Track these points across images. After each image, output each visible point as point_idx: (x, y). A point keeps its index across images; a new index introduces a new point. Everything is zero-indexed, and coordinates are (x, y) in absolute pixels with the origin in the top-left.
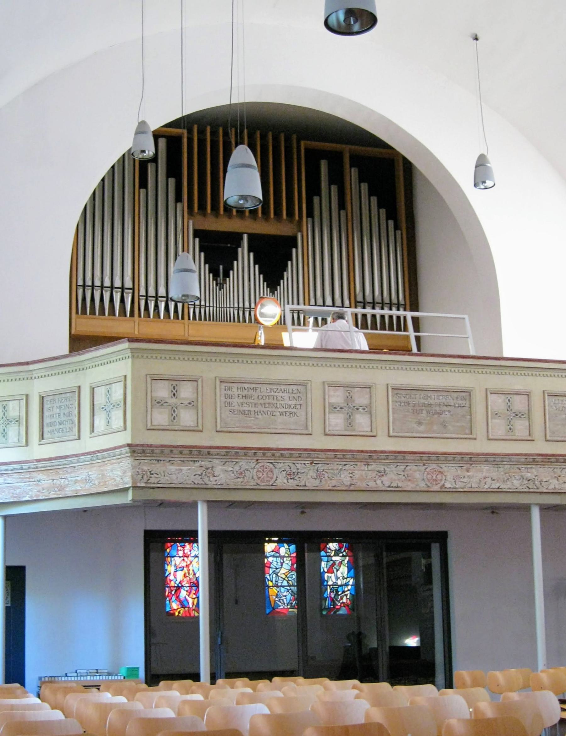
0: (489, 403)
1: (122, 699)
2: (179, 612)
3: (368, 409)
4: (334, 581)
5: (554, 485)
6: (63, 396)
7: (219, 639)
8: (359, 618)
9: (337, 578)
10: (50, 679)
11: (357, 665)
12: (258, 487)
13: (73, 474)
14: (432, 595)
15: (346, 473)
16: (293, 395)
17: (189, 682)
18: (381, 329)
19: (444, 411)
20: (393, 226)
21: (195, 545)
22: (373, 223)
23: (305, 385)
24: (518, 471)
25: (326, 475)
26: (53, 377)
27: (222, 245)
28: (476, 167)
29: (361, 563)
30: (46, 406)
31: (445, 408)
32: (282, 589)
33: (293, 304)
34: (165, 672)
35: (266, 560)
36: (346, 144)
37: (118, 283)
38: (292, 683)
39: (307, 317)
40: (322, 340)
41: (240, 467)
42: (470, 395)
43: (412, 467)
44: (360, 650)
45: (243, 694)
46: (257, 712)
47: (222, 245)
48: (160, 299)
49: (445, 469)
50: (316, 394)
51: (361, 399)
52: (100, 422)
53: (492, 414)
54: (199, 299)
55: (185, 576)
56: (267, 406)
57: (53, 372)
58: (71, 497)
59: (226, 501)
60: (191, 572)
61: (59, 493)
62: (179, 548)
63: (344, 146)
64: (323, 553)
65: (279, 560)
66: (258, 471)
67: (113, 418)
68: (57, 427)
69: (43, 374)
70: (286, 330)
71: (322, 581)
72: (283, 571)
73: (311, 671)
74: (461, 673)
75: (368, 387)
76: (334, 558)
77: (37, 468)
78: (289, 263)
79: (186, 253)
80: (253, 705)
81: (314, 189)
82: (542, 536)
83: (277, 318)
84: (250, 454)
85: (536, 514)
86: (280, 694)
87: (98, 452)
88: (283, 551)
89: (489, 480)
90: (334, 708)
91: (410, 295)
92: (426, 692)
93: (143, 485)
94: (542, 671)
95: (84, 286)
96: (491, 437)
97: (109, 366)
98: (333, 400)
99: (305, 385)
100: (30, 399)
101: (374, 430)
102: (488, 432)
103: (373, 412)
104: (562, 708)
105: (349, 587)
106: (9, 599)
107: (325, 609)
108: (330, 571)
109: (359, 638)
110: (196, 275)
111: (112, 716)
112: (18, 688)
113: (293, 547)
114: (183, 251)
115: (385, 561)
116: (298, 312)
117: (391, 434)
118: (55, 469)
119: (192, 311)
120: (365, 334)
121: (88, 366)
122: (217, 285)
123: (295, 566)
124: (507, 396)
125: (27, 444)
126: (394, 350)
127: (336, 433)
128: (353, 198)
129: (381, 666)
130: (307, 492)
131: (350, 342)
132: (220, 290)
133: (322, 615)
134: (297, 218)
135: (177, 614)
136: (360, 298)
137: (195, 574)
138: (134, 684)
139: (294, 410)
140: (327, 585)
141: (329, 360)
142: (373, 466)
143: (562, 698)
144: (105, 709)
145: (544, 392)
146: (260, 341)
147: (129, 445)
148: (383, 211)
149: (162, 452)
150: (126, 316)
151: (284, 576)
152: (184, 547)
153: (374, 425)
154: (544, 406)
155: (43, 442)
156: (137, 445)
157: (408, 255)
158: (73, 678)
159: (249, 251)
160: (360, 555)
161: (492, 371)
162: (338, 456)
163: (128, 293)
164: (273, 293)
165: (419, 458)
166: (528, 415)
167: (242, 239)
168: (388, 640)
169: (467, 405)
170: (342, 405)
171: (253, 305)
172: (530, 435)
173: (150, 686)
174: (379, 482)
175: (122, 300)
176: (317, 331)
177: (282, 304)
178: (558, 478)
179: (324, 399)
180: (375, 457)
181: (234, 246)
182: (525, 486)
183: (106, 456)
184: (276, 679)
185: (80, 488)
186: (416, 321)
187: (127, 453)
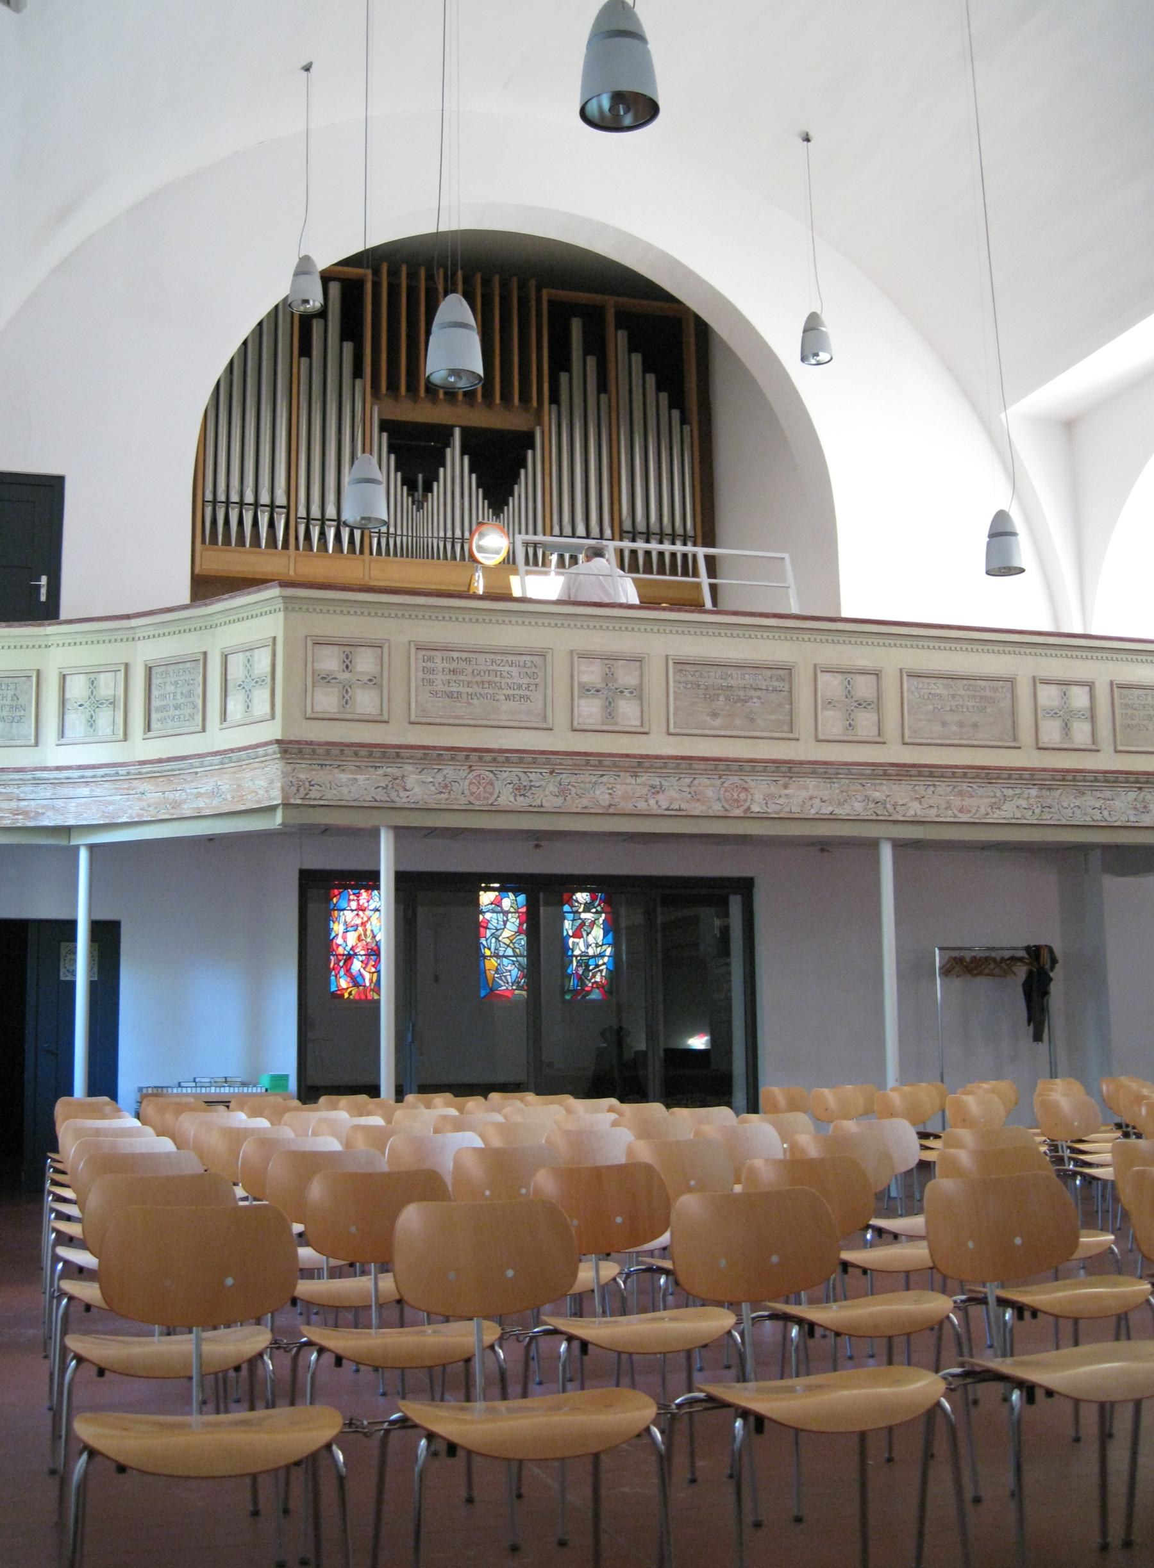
0: (819, 687)
1: (263, 1123)
2: (350, 994)
3: (638, 693)
4: (583, 949)
5: (915, 810)
6: (181, 666)
7: (410, 1035)
8: (619, 1006)
9: (588, 946)
10: (155, 1091)
11: (616, 1077)
12: (470, 807)
13: (193, 785)
14: (729, 973)
15: (603, 788)
16: (525, 670)
17: (363, 1098)
18: (659, 573)
19: (751, 698)
20: (678, 419)
21: (376, 892)
22: (649, 413)
23: (543, 655)
24: (860, 788)
25: (573, 790)
26: (166, 638)
27: (423, 444)
28: (805, 331)
29: (623, 923)
30: (156, 681)
31: (753, 693)
32: (505, 961)
33: (527, 533)
34: (327, 1083)
35: (481, 917)
36: (611, 294)
37: (265, 499)
38: (518, 1102)
39: (548, 553)
40: (569, 588)
41: (445, 777)
42: (791, 674)
43: (702, 780)
44: (620, 1054)
45: (444, 1118)
46: (465, 1145)
47: (423, 444)
48: (328, 523)
49: (752, 784)
50: (559, 667)
51: (627, 677)
52: (235, 706)
53: (823, 702)
54: (387, 524)
55: (359, 939)
56: (486, 685)
57: (166, 631)
58: (190, 818)
59: (423, 828)
60: (369, 933)
61: (172, 811)
62: (352, 897)
63: (606, 297)
64: (566, 908)
65: (501, 917)
66: (470, 784)
67: (255, 700)
68: (172, 712)
69: (151, 633)
70: (516, 572)
71: (564, 951)
72: (507, 933)
73: (546, 1082)
74: (771, 1089)
75: (638, 660)
76: (583, 916)
77: (140, 773)
78: (523, 471)
79: (367, 455)
80: (460, 1134)
81: (560, 362)
82: (895, 886)
83: (503, 554)
84: (459, 758)
85: (886, 854)
86: (499, 1118)
87: (232, 751)
88: (507, 903)
89: (817, 802)
90: (580, 1140)
91: (703, 522)
92: (718, 1119)
93: (299, 802)
94: (893, 1089)
95: (215, 502)
96: (821, 737)
97: (251, 622)
98: (585, 678)
99: (543, 655)
100: (132, 670)
101: (646, 724)
102: (816, 729)
103: (645, 696)
104: (921, 1145)
105: (606, 959)
106: (96, 970)
107: (569, 991)
108: (577, 934)
109: (619, 1036)
110: (382, 489)
111: (247, 1148)
112: (107, 1104)
113: (522, 898)
114: (364, 451)
115: (659, 920)
116: (535, 545)
117: (672, 730)
118: (168, 777)
119: (375, 541)
120: (634, 580)
121: (218, 622)
122: (413, 503)
123: (525, 926)
124: (846, 676)
125: (125, 739)
126: (678, 605)
127: (589, 728)
128: (620, 376)
129: (651, 1077)
130: (544, 816)
131: (612, 592)
132: (418, 510)
133: (564, 1001)
134: (535, 404)
135: (346, 995)
136: (627, 526)
137: (374, 937)
138: (280, 1099)
139: (527, 693)
140: (573, 956)
141: (579, 618)
142: (644, 778)
143: (922, 1130)
144: (237, 1136)
145: (901, 670)
146: (477, 588)
147: (278, 742)
148: (664, 396)
149: (328, 752)
150: (276, 548)
151: (507, 942)
152: (358, 895)
153: (646, 717)
154: (902, 692)
155: (149, 735)
156: (290, 742)
157: (701, 462)
158: (189, 1090)
159: (463, 453)
160: (623, 911)
161: (824, 638)
162: (592, 763)
163: (280, 514)
164: (498, 517)
165: (712, 767)
166: (877, 705)
167: (452, 434)
168: (662, 1039)
169: (786, 688)
170: (599, 686)
171: (467, 535)
172: (879, 735)
173: (304, 1103)
174: (652, 802)
175: (272, 524)
176: (562, 574)
177: (510, 534)
178: (920, 800)
179: (572, 677)
180: (647, 765)
181: (439, 445)
182: (871, 812)
183: (244, 757)
184: (494, 1096)
185: (206, 805)
186: (711, 561)
187: (275, 753)
